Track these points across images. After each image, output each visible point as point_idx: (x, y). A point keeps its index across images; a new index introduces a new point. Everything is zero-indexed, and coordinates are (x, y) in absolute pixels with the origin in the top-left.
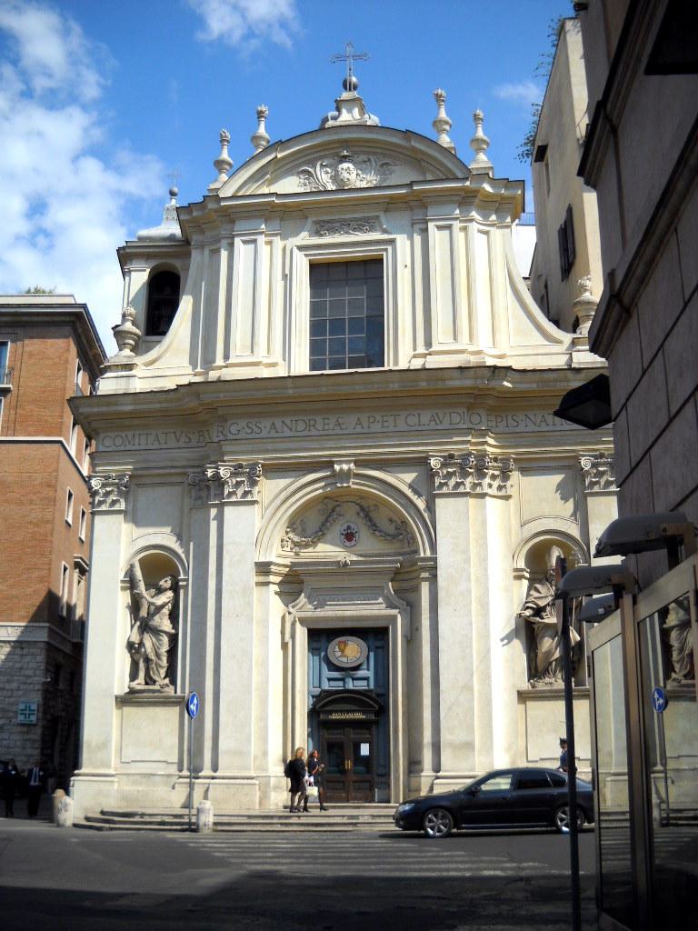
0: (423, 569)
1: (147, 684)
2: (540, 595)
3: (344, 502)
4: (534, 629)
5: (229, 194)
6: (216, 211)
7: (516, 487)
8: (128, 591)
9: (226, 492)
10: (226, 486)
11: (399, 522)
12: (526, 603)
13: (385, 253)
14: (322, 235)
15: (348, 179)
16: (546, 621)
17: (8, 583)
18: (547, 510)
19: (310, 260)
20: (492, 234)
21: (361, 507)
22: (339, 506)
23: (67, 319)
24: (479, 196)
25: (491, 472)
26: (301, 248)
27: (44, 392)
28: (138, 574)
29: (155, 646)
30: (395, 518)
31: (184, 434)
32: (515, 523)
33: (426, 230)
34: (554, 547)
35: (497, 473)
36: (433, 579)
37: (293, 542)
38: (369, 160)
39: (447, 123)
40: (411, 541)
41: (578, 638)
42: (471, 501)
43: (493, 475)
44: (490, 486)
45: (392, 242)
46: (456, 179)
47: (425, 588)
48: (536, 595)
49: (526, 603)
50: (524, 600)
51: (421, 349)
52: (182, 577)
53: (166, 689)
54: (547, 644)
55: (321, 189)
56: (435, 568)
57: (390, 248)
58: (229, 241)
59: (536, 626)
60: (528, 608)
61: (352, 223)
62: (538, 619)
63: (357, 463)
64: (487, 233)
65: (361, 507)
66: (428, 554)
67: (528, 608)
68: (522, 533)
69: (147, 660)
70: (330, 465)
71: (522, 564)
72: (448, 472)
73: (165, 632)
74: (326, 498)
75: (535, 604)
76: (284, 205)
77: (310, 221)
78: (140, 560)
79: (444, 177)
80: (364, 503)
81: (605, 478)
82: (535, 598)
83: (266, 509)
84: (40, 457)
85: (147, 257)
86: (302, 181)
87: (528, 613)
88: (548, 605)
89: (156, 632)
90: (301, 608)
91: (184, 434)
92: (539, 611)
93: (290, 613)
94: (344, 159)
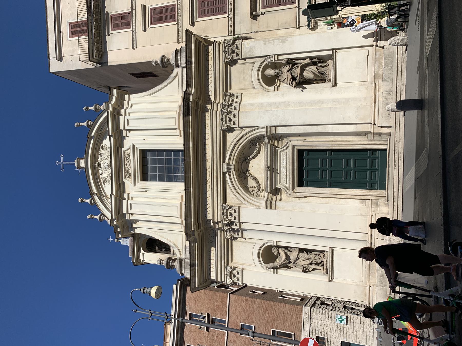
0: (271, 130)
1: (323, 265)
2: (286, 79)
3: (241, 169)
4: (303, 81)
5: (110, 215)
6: (118, 221)
7: (238, 91)
8: (279, 270)
10: (232, 221)
11: (251, 144)
12: (289, 84)
13: (138, 149)
14: (130, 176)
15: (107, 163)
16: (298, 75)
17: (286, 322)
18: (248, 77)
19: (141, 181)
20: (132, 103)
21: (244, 161)
22: (243, 171)
23: (182, 288)
24: (116, 107)
25: (230, 102)
27: (210, 300)
28: (271, 265)
29: (303, 260)
30: (249, 146)
31: (210, 239)
32: (254, 91)
33: (129, 130)
34: (265, 73)
35: (231, 100)
37: (257, 192)
38: (100, 154)
39: (88, 122)
40: (259, 138)
41: (308, 59)
42: (241, 110)
43: (231, 101)
44: (236, 102)
45: (134, 145)
48: (286, 79)
49: (289, 84)
50: (289, 85)
52: (272, 244)
53: (326, 256)
54: (308, 74)
57: (136, 146)
58: (131, 215)
59: (301, 80)
60: (292, 83)
61: (126, 162)
62: (298, 79)
64: (132, 105)
65: (244, 161)
66: (265, 130)
67: (292, 83)
68: (258, 88)
69: (311, 264)
70: (224, 174)
71: (272, 88)
72: (229, 121)
73: (298, 254)
74: (239, 176)
75: (290, 80)
76: (117, 192)
77: (124, 180)
78: (265, 264)
79: (107, 122)
80: (242, 160)
81: (235, 49)
82: (288, 81)
83: (242, 203)
84: (235, 303)
85: (139, 252)
86: (108, 183)
87: (294, 83)
88: (291, 74)
90: (288, 189)
91: (210, 239)
92: (294, 78)
93: (290, 194)
94: (99, 165)
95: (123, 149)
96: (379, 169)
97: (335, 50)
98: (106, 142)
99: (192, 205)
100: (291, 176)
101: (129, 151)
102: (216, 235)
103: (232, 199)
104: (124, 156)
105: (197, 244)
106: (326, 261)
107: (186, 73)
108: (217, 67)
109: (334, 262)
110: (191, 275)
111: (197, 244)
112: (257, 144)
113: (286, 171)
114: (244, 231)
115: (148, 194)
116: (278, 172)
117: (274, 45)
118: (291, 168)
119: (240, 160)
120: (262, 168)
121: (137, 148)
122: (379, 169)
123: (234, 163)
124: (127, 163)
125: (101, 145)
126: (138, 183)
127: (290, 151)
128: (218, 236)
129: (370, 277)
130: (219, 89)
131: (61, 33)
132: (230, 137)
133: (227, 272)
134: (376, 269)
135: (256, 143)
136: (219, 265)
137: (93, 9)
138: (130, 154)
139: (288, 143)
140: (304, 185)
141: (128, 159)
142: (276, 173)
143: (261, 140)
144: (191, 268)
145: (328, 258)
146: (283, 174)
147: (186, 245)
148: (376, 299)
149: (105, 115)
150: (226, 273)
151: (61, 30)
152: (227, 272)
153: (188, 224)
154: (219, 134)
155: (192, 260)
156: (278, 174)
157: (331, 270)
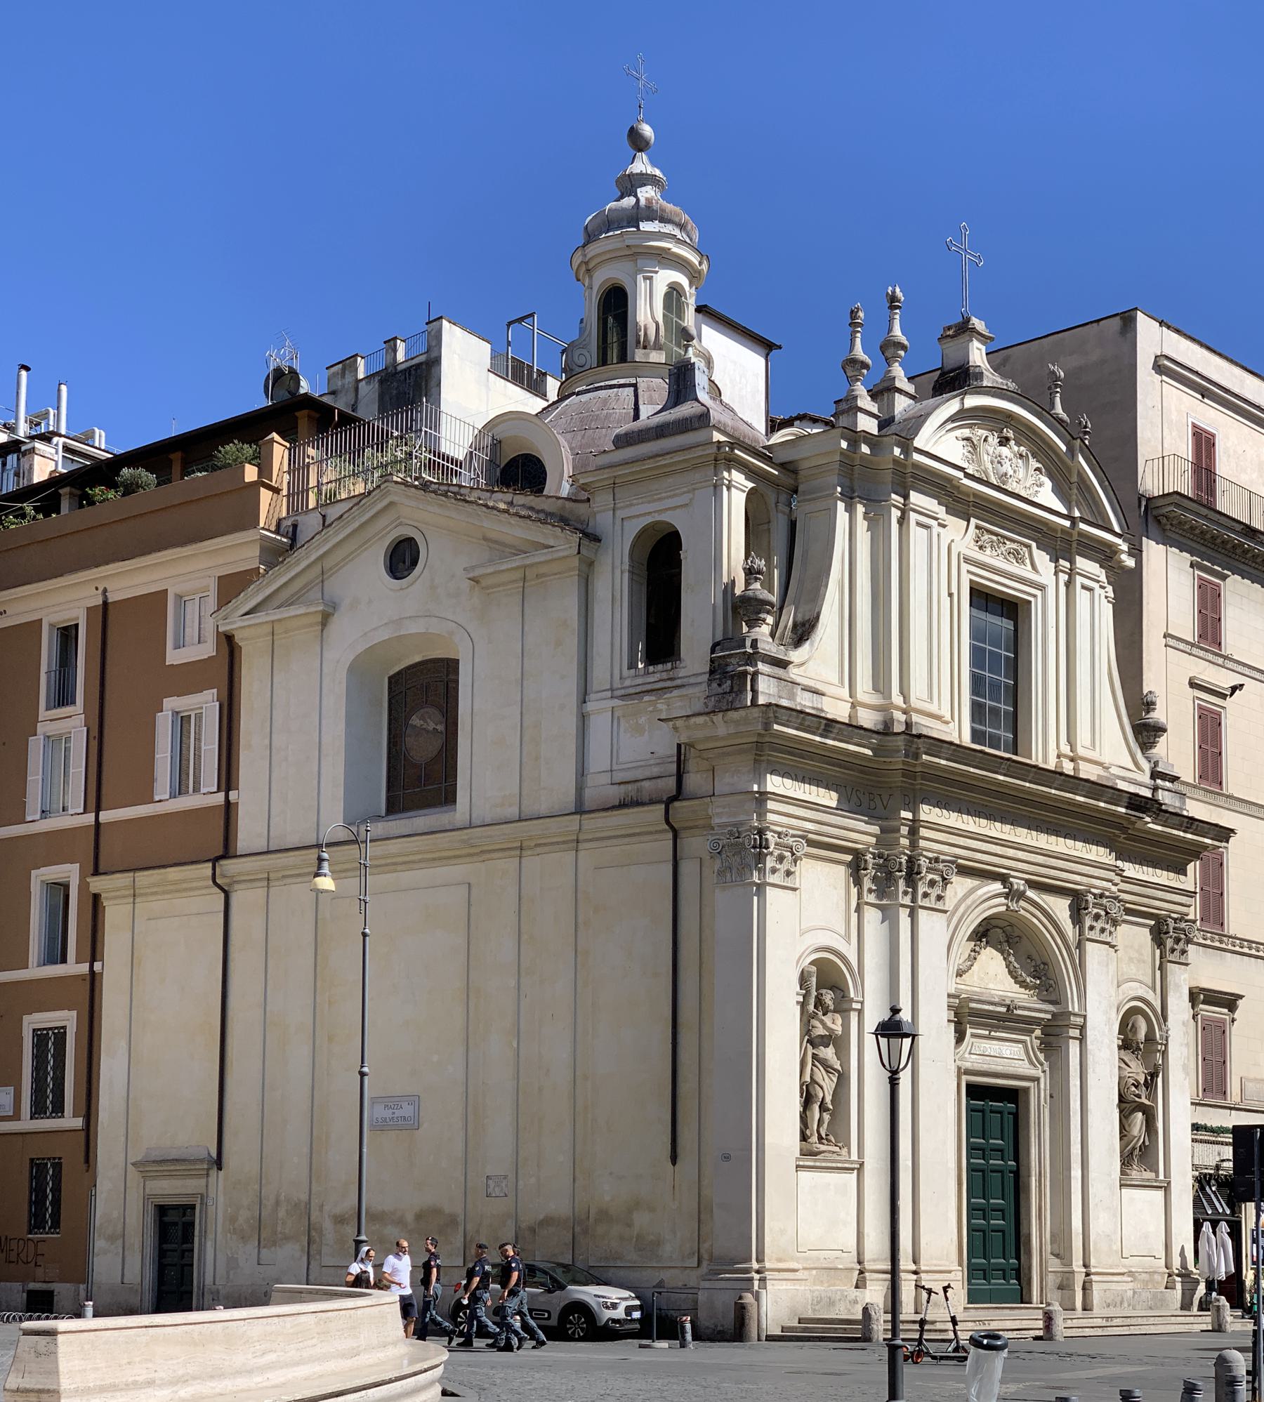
0: (1075, 1026)
9: (920, 892)
11: (1039, 963)
14: (981, 548)
26: (968, 560)
30: (1035, 956)
36: (1082, 1039)
46: (1111, 531)
47: (1074, 1047)
48: (1129, 1070)
51: (1066, 749)
55: (985, 479)
56: (1083, 1028)
63: (1027, 881)
89: (828, 1067)
94: (1004, 441)
95: (1034, 545)
96: (991, 1287)
97: (1167, 1189)
98: (1046, 495)
99: (972, 770)
100: (985, 1067)
101: (1029, 567)
102: (872, 817)
103: (959, 885)
104: (1018, 542)
105: (869, 752)
106: (834, 1152)
107: (1197, 817)
108: (1160, 894)
109: (830, 1172)
110: (810, 717)
111: (869, 752)
112: (1038, 982)
113: (992, 1054)
114: (880, 912)
115: (946, 600)
116: (993, 1033)
117: (1182, 1045)
118: (999, 1069)
119: (1011, 925)
120: (991, 986)
121: (1035, 596)
122: (991, 1287)
123: (1022, 912)
124: (1007, 547)
125: (1043, 470)
126: (968, 572)
127: (1025, 1068)
128: (866, 823)
129: (814, 1272)
130: (1128, 890)
131: (1200, 397)
132: (1060, 907)
133: (793, 836)
134: (829, 1286)
135: (1039, 978)
136: (806, 813)
137: (1248, 544)
138: (1023, 566)
139: (1042, 1064)
140: (972, 1100)
141: (1013, 554)
142: (992, 1027)
143: (1045, 993)
144: (824, 722)
145: (839, 1158)
146: (987, 1046)
147: (823, 695)
148: (784, 1287)
149: (1117, 529)
150: (791, 832)
151: (1206, 400)
152: (793, 836)
153: (942, 747)
154: (1077, 881)
155: (840, 729)
156: (987, 1032)
157: (818, 1164)
